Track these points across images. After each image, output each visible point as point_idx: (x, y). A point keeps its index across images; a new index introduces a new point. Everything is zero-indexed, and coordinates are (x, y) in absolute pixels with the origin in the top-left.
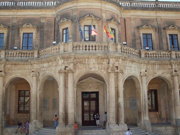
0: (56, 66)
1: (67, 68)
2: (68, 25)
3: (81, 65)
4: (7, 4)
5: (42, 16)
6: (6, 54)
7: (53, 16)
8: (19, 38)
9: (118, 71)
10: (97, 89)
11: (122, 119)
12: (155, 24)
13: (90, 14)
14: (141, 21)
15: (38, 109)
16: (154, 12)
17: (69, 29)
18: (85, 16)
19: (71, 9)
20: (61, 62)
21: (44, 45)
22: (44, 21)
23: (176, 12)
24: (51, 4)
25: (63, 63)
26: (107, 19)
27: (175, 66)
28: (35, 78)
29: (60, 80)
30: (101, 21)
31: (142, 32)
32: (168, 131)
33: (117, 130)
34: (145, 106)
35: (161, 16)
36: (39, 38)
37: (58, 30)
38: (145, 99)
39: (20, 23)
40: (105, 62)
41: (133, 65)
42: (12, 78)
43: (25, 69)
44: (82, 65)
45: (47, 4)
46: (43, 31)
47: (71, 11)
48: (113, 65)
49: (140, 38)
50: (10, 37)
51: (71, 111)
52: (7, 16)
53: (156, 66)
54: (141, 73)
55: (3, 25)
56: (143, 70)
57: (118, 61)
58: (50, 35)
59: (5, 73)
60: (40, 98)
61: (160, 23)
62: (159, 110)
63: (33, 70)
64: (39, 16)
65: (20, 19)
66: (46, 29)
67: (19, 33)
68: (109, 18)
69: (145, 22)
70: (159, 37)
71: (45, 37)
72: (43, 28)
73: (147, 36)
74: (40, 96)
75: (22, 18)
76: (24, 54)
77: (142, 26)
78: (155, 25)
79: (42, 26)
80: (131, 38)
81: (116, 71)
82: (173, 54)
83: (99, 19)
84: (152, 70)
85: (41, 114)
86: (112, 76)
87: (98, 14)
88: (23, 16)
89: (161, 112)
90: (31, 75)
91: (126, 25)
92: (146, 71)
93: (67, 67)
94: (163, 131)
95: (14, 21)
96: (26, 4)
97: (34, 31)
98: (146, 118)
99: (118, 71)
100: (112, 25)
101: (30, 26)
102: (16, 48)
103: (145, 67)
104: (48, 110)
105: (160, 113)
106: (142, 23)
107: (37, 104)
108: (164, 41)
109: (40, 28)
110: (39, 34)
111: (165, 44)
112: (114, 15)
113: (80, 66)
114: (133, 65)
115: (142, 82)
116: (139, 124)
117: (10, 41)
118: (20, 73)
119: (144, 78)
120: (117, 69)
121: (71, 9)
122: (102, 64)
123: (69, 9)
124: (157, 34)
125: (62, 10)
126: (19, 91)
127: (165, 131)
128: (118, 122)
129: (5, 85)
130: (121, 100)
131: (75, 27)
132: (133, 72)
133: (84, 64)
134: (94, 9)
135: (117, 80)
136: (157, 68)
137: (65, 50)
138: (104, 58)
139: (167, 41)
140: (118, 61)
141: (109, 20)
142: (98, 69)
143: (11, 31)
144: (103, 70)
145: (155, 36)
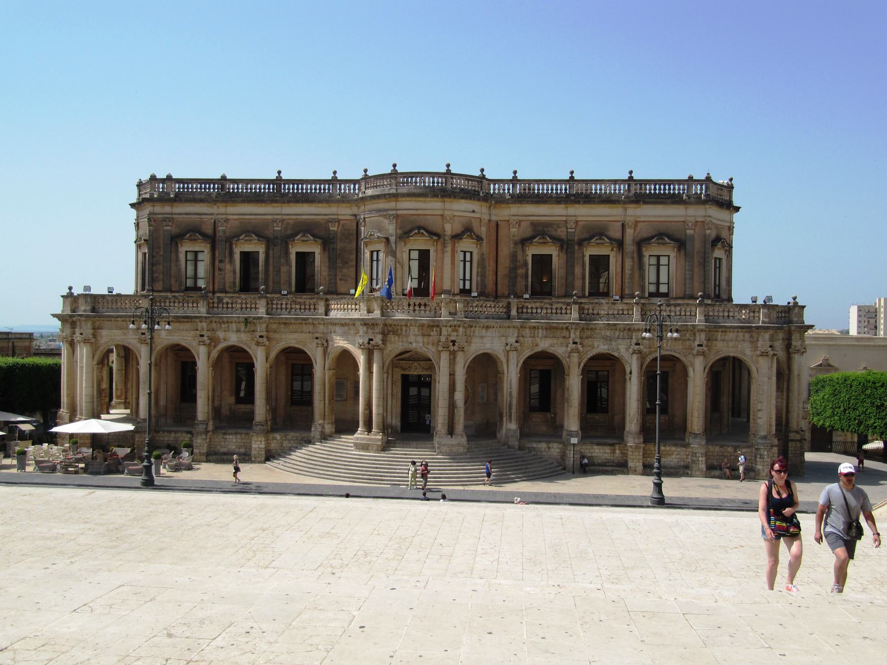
4: (260, 189)
6: (268, 304)
9: (456, 348)
10: (427, 370)
11: (460, 427)
12: (561, 233)
13: (419, 228)
15: (327, 402)
16: (563, 206)
20: (362, 330)
22: (335, 229)
23: (612, 206)
24: (349, 190)
25: (367, 333)
28: (320, 350)
29: (361, 359)
30: (442, 240)
32: (552, 450)
34: (510, 405)
38: (511, 392)
39: (289, 232)
41: (490, 332)
43: (302, 332)
44: (397, 338)
45: (340, 189)
49: (526, 264)
53: (540, 331)
55: (257, 235)
56: (512, 340)
57: (457, 331)
59: (268, 339)
60: (330, 383)
62: (552, 411)
63: (317, 335)
65: (288, 224)
66: (339, 245)
67: (287, 253)
68: (458, 229)
69: (541, 228)
73: (543, 263)
76: (300, 304)
81: (452, 348)
83: (435, 235)
84: (530, 339)
87: (435, 224)
89: (555, 414)
90: (314, 345)
92: (517, 342)
93: (372, 340)
97: (316, 249)
98: (510, 426)
99: (456, 348)
100: (466, 244)
102: (285, 292)
103: (516, 335)
104: (346, 400)
108: (578, 270)
109: (327, 242)
111: (580, 276)
113: (392, 337)
114: (489, 334)
115: (508, 361)
116: (498, 435)
117: (271, 268)
119: (513, 355)
120: (454, 345)
124: (563, 256)
126: (293, 365)
128: (451, 431)
130: (459, 396)
132: (488, 346)
133: (399, 335)
135: (452, 362)
136: (540, 335)
137: (371, 309)
138: (433, 326)
139: (584, 270)
141: (457, 237)
144: (430, 346)
145: (558, 261)
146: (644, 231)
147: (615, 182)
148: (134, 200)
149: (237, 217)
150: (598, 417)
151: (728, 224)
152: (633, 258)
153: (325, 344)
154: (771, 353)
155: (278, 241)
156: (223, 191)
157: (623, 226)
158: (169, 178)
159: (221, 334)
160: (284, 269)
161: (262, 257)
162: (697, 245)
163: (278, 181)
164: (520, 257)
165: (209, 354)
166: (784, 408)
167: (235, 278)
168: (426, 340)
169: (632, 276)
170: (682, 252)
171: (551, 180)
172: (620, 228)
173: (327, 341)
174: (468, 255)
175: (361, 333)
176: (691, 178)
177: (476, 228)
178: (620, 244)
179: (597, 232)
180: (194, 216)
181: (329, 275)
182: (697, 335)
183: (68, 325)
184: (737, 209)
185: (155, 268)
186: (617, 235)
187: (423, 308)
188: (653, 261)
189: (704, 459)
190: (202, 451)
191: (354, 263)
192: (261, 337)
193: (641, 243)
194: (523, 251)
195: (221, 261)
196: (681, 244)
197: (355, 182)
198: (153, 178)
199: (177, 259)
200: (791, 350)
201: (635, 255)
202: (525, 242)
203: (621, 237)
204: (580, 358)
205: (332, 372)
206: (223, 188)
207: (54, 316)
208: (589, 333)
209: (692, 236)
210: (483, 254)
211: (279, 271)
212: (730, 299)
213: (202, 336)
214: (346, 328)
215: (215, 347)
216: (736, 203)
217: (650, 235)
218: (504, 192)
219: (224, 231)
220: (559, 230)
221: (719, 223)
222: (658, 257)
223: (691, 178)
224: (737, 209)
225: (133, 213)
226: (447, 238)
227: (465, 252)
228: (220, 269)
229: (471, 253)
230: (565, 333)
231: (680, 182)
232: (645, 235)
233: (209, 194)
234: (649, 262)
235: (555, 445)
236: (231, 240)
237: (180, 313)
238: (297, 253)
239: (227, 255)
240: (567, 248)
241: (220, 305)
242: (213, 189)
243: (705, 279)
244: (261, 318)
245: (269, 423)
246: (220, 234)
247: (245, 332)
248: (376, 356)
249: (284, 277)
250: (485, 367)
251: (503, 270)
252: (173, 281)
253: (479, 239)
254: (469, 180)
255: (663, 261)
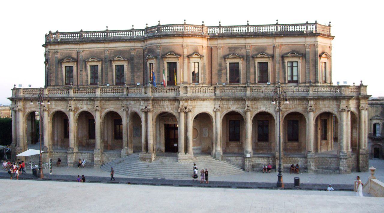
0: (139, 105)
1: (146, 108)
2: (154, 61)
3: (157, 105)
5: (131, 48)
7: (142, 47)
8: (112, 71)
12: (243, 52)
13: (171, 52)
14: (229, 50)
15: (129, 138)
17: (155, 66)
18: (167, 54)
19: (155, 45)
20: (142, 103)
21: (135, 77)
22: (134, 53)
26: (188, 54)
27: (248, 102)
28: (125, 113)
29: (143, 116)
30: (182, 57)
31: (228, 61)
33: (184, 158)
35: (250, 42)
36: (130, 70)
37: (146, 65)
39: (112, 55)
40: (176, 103)
41: (205, 103)
42: (107, 111)
43: (116, 104)
44: (158, 106)
45: (136, 34)
46: (133, 63)
47: (155, 47)
48: (182, 106)
49: (226, 68)
50: (104, 69)
51: (151, 142)
52: (100, 48)
54: (215, 108)
56: (217, 107)
58: (140, 67)
59: (101, 107)
61: (249, 50)
63: (123, 106)
64: (130, 48)
66: (136, 61)
67: (111, 66)
68: (191, 52)
69: (233, 50)
70: (246, 66)
71: (135, 69)
72: (133, 60)
74: (130, 127)
75: (113, 50)
77: (229, 55)
78: (243, 53)
79: (133, 57)
80: (217, 68)
81: (185, 110)
82: (248, 90)
83: (178, 55)
84: (226, 105)
85: (131, 142)
86: (183, 115)
87: (179, 50)
88: (114, 48)
89: (242, 143)
90: (122, 110)
91: (212, 55)
92: (219, 107)
94: (234, 160)
95: (106, 53)
96: (116, 35)
97: (125, 64)
99: (187, 110)
101: (121, 59)
105: (241, 143)
106: (230, 51)
107: (127, 134)
108: (252, 70)
109: (130, 60)
110: (130, 66)
112: (198, 48)
115: (215, 116)
116: (212, 153)
117: (104, 74)
118: (113, 107)
119: (218, 114)
121: (155, 45)
122: (174, 105)
123: (154, 45)
125: (149, 44)
127: (236, 160)
129: (101, 118)
131: (159, 64)
133: (159, 105)
134: (176, 46)
135: (186, 118)
136: (231, 103)
140: (187, 102)
141: (189, 57)
142: (170, 109)
143: (104, 63)
146: (285, 50)
147: (270, 25)
148: (44, 43)
149: (88, 49)
150: (263, 144)
151: (329, 45)
152: (279, 63)
153: (127, 109)
154: (347, 109)
155: (108, 61)
156: (81, 38)
157: (274, 47)
158: (57, 32)
159: (79, 107)
160: (110, 73)
161: (100, 68)
162: (311, 56)
163: (106, 32)
164: (223, 65)
165: (74, 115)
166: (358, 138)
167: (87, 78)
168: (172, 106)
169: (279, 72)
170: (304, 60)
171: (237, 26)
172: (272, 48)
173: (128, 108)
174: (197, 64)
175: (142, 104)
176: (307, 23)
177: (200, 52)
178: (273, 57)
179: (261, 51)
180: (68, 50)
181: (131, 76)
182: (309, 102)
183: (14, 104)
184: (333, 37)
185: (51, 75)
186: (270, 52)
187: (173, 91)
188: (289, 65)
189: (314, 164)
190: (71, 162)
191: (143, 70)
192: (97, 106)
193: (283, 57)
194: (225, 61)
195: (81, 71)
196: (303, 55)
197: (142, 30)
198: (50, 32)
199: (61, 70)
200: (360, 108)
201: (281, 62)
202: (225, 57)
203: (273, 54)
204: (251, 114)
205: (130, 124)
206: (81, 36)
207: (8, 98)
208: (255, 102)
209: (308, 52)
210: (204, 63)
211: (108, 75)
212: (331, 83)
213: (71, 107)
214: (135, 102)
215: (77, 112)
216: (332, 35)
217: (288, 52)
218: (215, 33)
219: (82, 56)
220: (242, 50)
221: (323, 44)
222: (292, 63)
223: (307, 23)
224: (333, 37)
225: (44, 48)
226: (185, 56)
227: (195, 63)
228: (80, 74)
229: (198, 63)
230: (243, 102)
231: (302, 25)
232: (286, 52)
233: (75, 39)
234: (287, 64)
235: (240, 158)
236: (85, 62)
237: (61, 95)
238: (116, 65)
239: (84, 67)
240: (247, 59)
241: (79, 92)
242: (77, 37)
243: (316, 73)
244: (97, 97)
245: (102, 148)
246: (80, 57)
247: (90, 105)
248: (150, 116)
249: (110, 77)
250: (204, 119)
251: (215, 71)
252: (59, 81)
253: (201, 57)
254: (195, 27)
255: (295, 64)
